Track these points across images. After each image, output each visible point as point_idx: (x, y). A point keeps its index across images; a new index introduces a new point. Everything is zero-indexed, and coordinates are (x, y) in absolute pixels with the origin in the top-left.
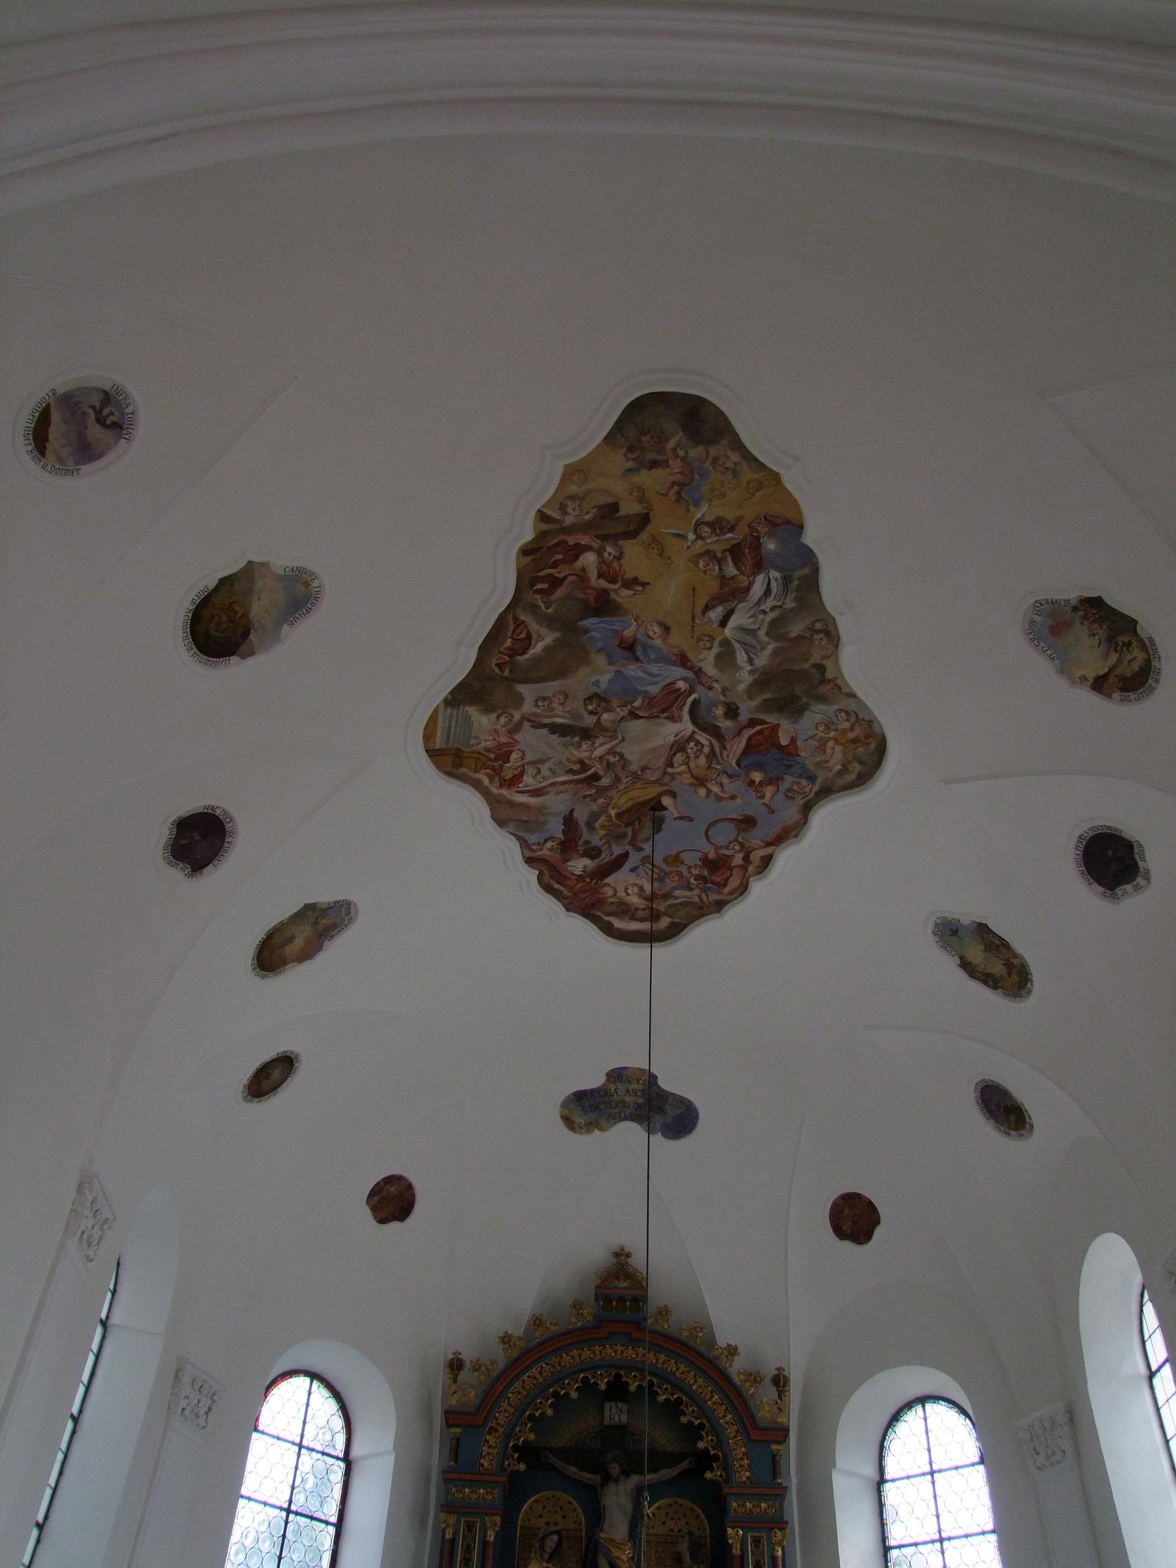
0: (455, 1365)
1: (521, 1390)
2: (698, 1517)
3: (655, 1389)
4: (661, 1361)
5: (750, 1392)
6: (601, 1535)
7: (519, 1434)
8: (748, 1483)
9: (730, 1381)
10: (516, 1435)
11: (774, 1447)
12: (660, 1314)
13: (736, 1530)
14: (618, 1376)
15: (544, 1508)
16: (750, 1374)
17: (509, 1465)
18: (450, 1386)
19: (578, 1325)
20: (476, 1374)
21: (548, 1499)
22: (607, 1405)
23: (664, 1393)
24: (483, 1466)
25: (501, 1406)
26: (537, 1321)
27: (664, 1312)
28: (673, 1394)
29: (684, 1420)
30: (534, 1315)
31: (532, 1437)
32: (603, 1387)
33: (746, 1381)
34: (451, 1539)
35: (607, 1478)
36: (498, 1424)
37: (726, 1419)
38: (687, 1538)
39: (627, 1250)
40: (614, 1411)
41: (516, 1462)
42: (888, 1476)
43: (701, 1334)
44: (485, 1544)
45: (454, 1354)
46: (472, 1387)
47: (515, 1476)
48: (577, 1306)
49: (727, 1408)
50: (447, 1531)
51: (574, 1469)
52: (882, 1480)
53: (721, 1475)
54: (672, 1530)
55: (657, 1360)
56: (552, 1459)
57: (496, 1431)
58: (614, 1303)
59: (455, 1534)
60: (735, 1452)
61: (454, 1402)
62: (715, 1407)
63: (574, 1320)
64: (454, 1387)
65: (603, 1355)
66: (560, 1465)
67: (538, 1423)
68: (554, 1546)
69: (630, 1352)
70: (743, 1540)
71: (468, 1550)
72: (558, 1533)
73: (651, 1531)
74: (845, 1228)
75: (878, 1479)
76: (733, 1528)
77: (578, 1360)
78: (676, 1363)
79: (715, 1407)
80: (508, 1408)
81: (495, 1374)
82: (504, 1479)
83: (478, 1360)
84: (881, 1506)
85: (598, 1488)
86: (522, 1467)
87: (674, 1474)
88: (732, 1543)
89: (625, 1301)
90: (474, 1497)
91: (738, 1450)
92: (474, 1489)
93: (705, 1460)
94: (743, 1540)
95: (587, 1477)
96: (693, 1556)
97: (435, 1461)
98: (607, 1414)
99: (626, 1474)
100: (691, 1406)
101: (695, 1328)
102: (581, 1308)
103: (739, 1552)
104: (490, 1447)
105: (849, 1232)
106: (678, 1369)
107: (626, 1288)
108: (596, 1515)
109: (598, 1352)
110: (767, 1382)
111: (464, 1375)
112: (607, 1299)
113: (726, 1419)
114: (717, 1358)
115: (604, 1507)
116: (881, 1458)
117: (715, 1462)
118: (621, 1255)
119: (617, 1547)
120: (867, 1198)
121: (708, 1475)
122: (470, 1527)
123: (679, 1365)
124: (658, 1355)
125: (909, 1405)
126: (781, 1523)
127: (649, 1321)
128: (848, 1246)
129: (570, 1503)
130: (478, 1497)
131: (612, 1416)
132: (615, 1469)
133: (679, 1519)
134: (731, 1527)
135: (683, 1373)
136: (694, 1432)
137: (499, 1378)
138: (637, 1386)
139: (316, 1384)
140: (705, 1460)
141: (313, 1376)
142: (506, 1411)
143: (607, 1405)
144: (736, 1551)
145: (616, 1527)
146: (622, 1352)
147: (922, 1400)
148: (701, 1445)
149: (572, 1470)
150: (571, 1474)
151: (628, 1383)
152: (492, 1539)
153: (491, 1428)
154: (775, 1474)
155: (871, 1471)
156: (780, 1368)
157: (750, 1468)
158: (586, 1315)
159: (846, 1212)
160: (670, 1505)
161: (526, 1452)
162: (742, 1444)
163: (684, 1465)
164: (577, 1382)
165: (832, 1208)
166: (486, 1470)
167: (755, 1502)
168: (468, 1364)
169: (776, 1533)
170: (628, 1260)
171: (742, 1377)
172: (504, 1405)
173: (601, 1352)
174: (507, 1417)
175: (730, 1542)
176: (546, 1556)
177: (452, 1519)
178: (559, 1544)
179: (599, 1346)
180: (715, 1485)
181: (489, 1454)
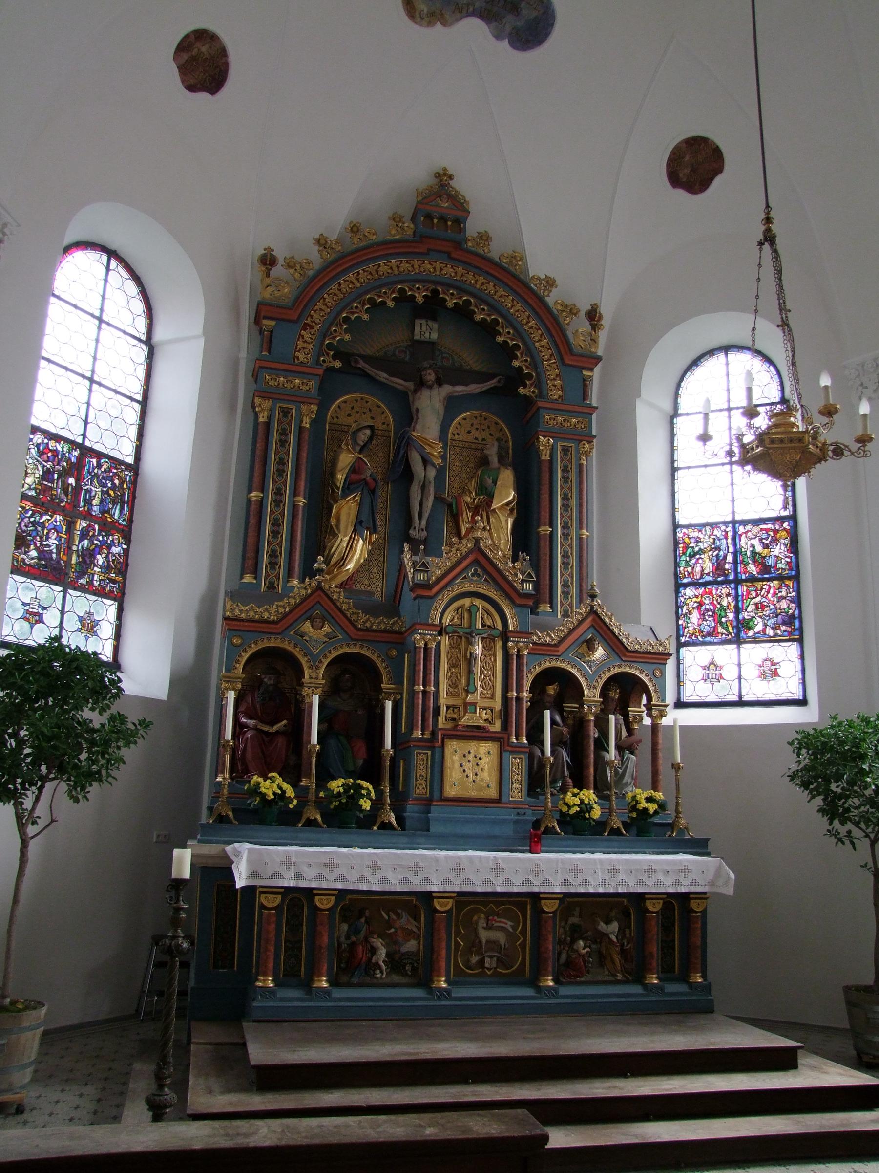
0: (268, 261)
1: (338, 292)
2: (501, 430)
3: (472, 308)
4: (480, 283)
5: (567, 322)
6: (413, 433)
7: (335, 335)
8: (560, 400)
10: (331, 334)
11: (585, 373)
12: (481, 238)
13: (547, 439)
14: (435, 292)
15: (352, 408)
16: (567, 305)
17: (324, 361)
18: (262, 280)
19: (398, 237)
20: (291, 271)
21: (357, 401)
22: (418, 322)
23: (481, 313)
24: (298, 358)
25: (316, 305)
26: (354, 229)
27: (484, 237)
28: (489, 315)
30: (351, 222)
31: (347, 337)
32: (420, 299)
33: (563, 311)
34: (264, 422)
35: (421, 384)
36: (314, 322)
37: (542, 343)
38: (496, 444)
39: (450, 173)
40: (424, 328)
41: (331, 360)
42: (680, 411)
43: (520, 263)
44: (301, 430)
45: (265, 249)
46: (287, 283)
47: (331, 370)
48: (396, 219)
49: (542, 334)
50: (261, 415)
51: (385, 375)
52: (675, 414)
53: (533, 392)
54: (476, 439)
55: (476, 281)
56: (362, 364)
57: (312, 327)
58: (435, 221)
59: (270, 418)
60: (549, 373)
61: (267, 294)
62: (531, 331)
63: (394, 232)
64: (267, 281)
65: (422, 269)
66: (372, 371)
67: (353, 326)
68: (366, 439)
69: (449, 270)
70: (553, 449)
71: (284, 433)
72: (371, 428)
73: (456, 437)
74: (681, 175)
75: (672, 413)
76: (545, 437)
77: (396, 272)
78: (494, 286)
79: (531, 331)
80: (324, 307)
81: (310, 273)
82: (321, 372)
83: (293, 257)
84: (672, 435)
85: (410, 393)
87: (484, 389)
88: (542, 450)
89: (446, 222)
90: (289, 386)
91: (551, 370)
92: (290, 378)
94: (553, 449)
95: (398, 383)
96: (501, 459)
97: (243, 354)
98: (417, 330)
99: (439, 383)
100: (507, 327)
101: (515, 257)
102: (400, 221)
103: (548, 458)
104: (305, 342)
105: (684, 180)
106: (496, 292)
107: (446, 207)
109: (416, 266)
110: (582, 314)
111: (278, 271)
112: (429, 217)
113: (542, 343)
115: (417, 410)
116: (676, 395)
117: (528, 380)
118: (443, 179)
119: (429, 445)
120: (714, 143)
121: (522, 390)
122: (286, 412)
123: (498, 288)
124: (477, 277)
125: (711, 353)
127: (470, 244)
129: (379, 406)
130: (294, 386)
131: (423, 333)
132: (430, 377)
133: (484, 430)
134: (543, 436)
135: (501, 296)
136: (508, 352)
137: (315, 277)
138: (454, 303)
139: (114, 263)
140: (519, 377)
141: (112, 254)
142: (321, 310)
143: (418, 322)
144: (545, 456)
146: (441, 269)
147: (726, 349)
148: (516, 363)
149: (383, 376)
150: (382, 379)
151: (445, 300)
152: (308, 426)
153: (306, 324)
155: (667, 406)
156: (596, 304)
157: (562, 388)
158: (406, 228)
159: (687, 158)
160: (476, 418)
162: (556, 367)
163: (492, 383)
164: (393, 292)
165: (673, 153)
166: (301, 362)
167: (567, 418)
168: (281, 261)
169: (584, 444)
170: (451, 182)
171: (559, 308)
172: (320, 305)
173: (420, 267)
174: (323, 316)
175: (541, 448)
176: (358, 448)
177: (267, 404)
178: (371, 439)
179: (418, 261)
180: (528, 401)
181: (304, 348)
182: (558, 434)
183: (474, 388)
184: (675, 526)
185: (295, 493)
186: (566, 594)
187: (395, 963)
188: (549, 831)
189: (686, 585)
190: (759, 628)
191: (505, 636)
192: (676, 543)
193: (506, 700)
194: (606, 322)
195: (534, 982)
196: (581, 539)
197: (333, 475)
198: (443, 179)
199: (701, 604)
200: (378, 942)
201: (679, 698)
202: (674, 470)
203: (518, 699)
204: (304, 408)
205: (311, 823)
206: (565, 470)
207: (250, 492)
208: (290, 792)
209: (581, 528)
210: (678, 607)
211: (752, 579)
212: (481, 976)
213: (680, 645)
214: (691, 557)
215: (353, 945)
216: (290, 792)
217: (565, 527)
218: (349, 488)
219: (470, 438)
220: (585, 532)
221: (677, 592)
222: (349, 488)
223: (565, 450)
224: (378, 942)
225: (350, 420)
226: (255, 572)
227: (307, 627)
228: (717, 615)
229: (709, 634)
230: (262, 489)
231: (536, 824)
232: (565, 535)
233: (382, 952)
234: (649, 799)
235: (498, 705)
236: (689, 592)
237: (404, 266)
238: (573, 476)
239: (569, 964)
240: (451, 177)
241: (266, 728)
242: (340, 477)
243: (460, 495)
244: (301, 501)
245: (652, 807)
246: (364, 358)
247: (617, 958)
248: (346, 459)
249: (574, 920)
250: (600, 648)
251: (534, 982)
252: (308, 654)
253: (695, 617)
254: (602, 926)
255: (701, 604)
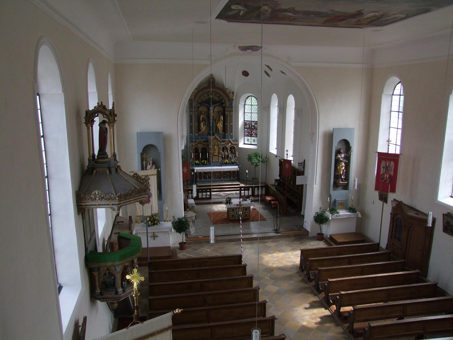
9: (226, 93)
27: (218, 83)
29: (220, 98)
37: (226, 98)
44: (196, 115)
52: (245, 105)
59: (192, 114)
70: (228, 113)
84: (245, 108)
86: (200, 105)
91: (227, 102)
93: (223, 103)
95: (208, 105)
96: (221, 114)
108: (209, 110)
110: (232, 93)
113: (226, 98)
114: (225, 90)
116: (245, 102)
121: (223, 105)
125: (250, 96)
126: (232, 111)
128: (244, 77)
140: (223, 103)
144: (227, 114)
145: (211, 111)
147: (252, 96)
149: (205, 104)
154: (232, 105)
155: (244, 104)
161: (200, 103)
172: (197, 98)
182: (228, 111)
183: (217, 104)
184: (245, 121)
185: (196, 123)
186: (229, 132)
187: (209, 177)
188: (224, 164)
189: (245, 129)
190: (253, 135)
191: (219, 145)
192: (244, 123)
193: (219, 152)
194: (235, 94)
195: (221, 178)
196: (231, 125)
197: (200, 120)
198: (212, 75)
199: (247, 131)
200: (207, 176)
201: (244, 143)
202: (245, 113)
203: (220, 152)
204: (196, 113)
205: (201, 165)
206: (229, 116)
207: (191, 124)
208: (199, 162)
209: (231, 123)
210: (245, 131)
211: (253, 129)
212: (216, 178)
213: (245, 136)
214: (246, 125)
215: (205, 176)
216: (199, 162)
217: (229, 123)
218: (202, 121)
219: (217, 110)
220: (232, 124)
221: (244, 129)
222: (202, 121)
223: (229, 113)
224: (207, 176)
225: (202, 110)
226: (192, 134)
227: (199, 145)
228: (249, 133)
229: (248, 135)
230: (192, 123)
231: (222, 164)
232: (229, 125)
233: (207, 176)
234: (234, 161)
235: (218, 152)
236: (246, 129)
237: (207, 90)
238: (230, 116)
239: (224, 177)
240: (213, 75)
241: (196, 154)
242: (201, 119)
243: (216, 119)
244: (197, 124)
245: (234, 161)
246: (203, 101)
247: (228, 176)
248: (201, 117)
249: (224, 173)
250: (230, 144)
251: (221, 178)
252: (199, 147)
253: (246, 133)
254: (227, 174)
255: (247, 131)
